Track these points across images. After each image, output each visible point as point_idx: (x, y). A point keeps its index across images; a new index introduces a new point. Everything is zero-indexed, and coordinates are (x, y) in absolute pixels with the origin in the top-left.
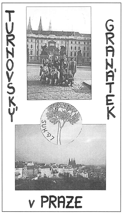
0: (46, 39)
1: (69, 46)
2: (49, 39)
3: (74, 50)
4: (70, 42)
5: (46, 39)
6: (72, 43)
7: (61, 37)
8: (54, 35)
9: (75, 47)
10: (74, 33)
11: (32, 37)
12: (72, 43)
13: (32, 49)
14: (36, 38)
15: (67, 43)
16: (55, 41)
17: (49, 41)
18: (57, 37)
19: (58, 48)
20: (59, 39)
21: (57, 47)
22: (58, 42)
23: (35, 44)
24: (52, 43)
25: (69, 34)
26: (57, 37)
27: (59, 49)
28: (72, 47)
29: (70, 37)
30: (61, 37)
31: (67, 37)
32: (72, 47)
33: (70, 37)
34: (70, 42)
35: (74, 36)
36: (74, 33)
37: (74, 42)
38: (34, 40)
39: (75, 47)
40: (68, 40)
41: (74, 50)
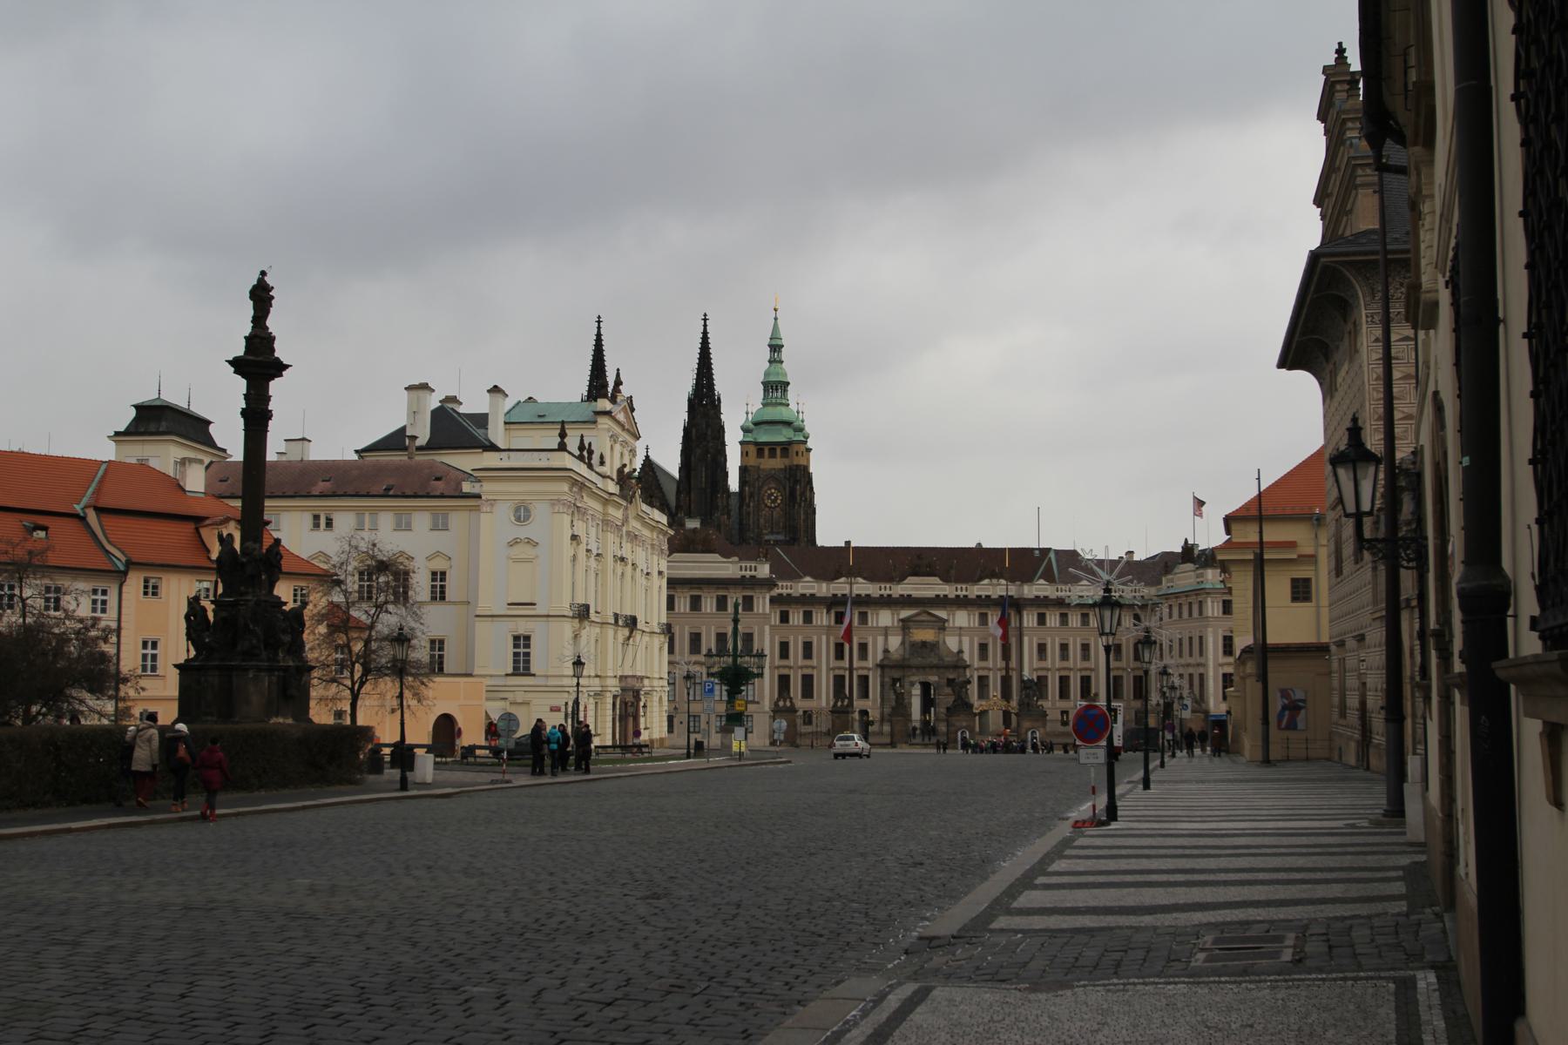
0: (887, 602)
1: (1026, 639)
2: (907, 601)
3: (1053, 662)
4: (1029, 619)
5: (887, 602)
6: (1042, 619)
7: (975, 591)
8: (936, 580)
9: (1064, 647)
10: (1052, 555)
11: (808, 601)
12: (1042, 619)
13: (814, 662)
14: (835, 604)
15: (1014, 623)
16: (942, 614)
17: (905, 613)
18: (948, 590)
19: (961, 651)
20: (962, 603)
21: (955, 650)
22: (962, 618)
23: (824, 638)
24: (921, 624)
25: (1025, 563)
26: (948, 590)
27: (966, 656)
28: (1042, 649)
29: (1030, 591)
30: (975, 591)
31: (1013, 590)
32: (1042, 649)
33: (1030, 591)
34: (1029, 619)
35: (1049, 577)
36: (1052, 555)
37: (1053, 619)
38: (822, 618)
39: (1064, 647)
40: (1018, 605)
41: (1053, 662)
